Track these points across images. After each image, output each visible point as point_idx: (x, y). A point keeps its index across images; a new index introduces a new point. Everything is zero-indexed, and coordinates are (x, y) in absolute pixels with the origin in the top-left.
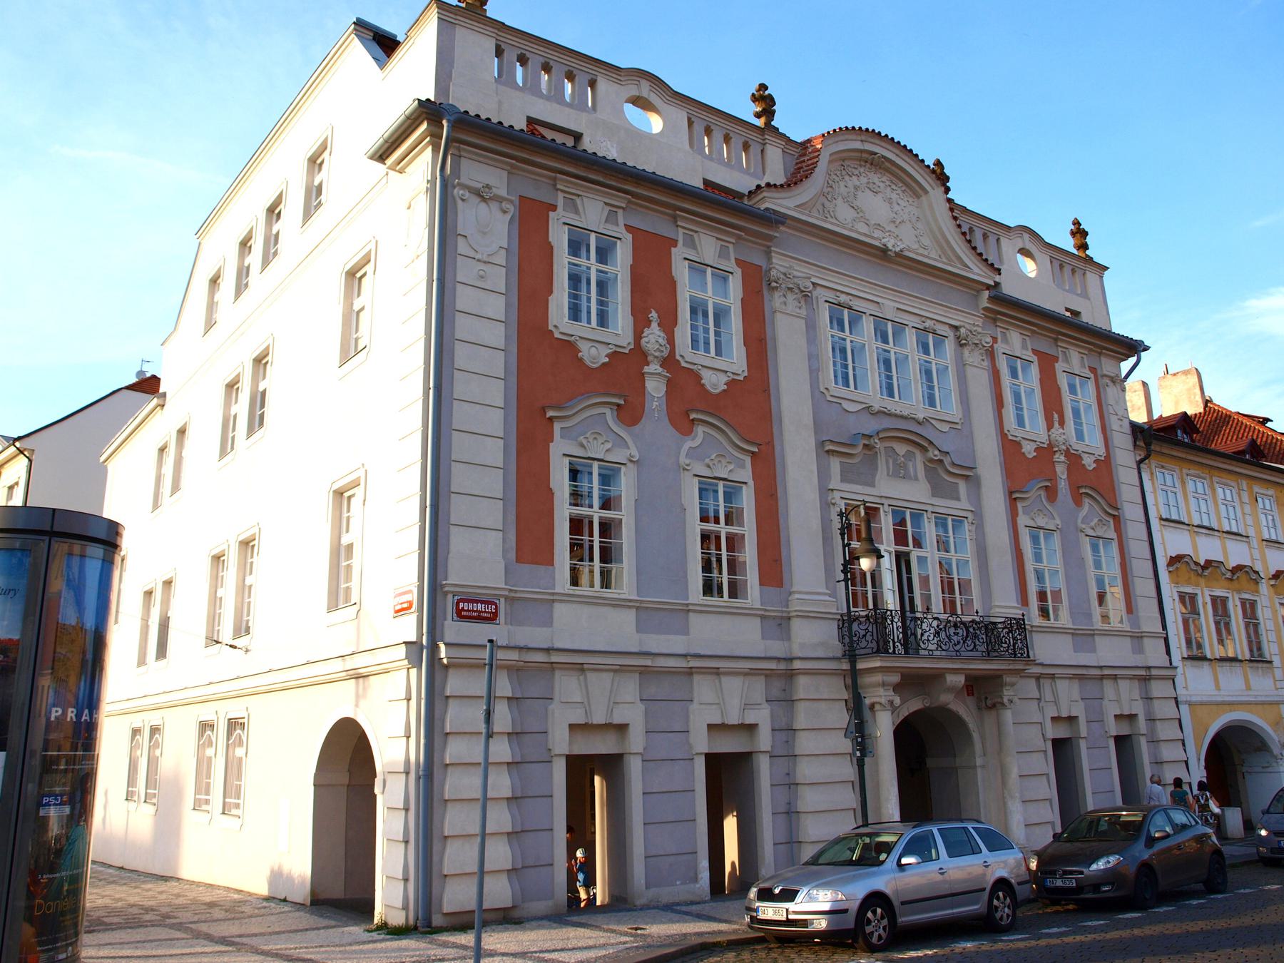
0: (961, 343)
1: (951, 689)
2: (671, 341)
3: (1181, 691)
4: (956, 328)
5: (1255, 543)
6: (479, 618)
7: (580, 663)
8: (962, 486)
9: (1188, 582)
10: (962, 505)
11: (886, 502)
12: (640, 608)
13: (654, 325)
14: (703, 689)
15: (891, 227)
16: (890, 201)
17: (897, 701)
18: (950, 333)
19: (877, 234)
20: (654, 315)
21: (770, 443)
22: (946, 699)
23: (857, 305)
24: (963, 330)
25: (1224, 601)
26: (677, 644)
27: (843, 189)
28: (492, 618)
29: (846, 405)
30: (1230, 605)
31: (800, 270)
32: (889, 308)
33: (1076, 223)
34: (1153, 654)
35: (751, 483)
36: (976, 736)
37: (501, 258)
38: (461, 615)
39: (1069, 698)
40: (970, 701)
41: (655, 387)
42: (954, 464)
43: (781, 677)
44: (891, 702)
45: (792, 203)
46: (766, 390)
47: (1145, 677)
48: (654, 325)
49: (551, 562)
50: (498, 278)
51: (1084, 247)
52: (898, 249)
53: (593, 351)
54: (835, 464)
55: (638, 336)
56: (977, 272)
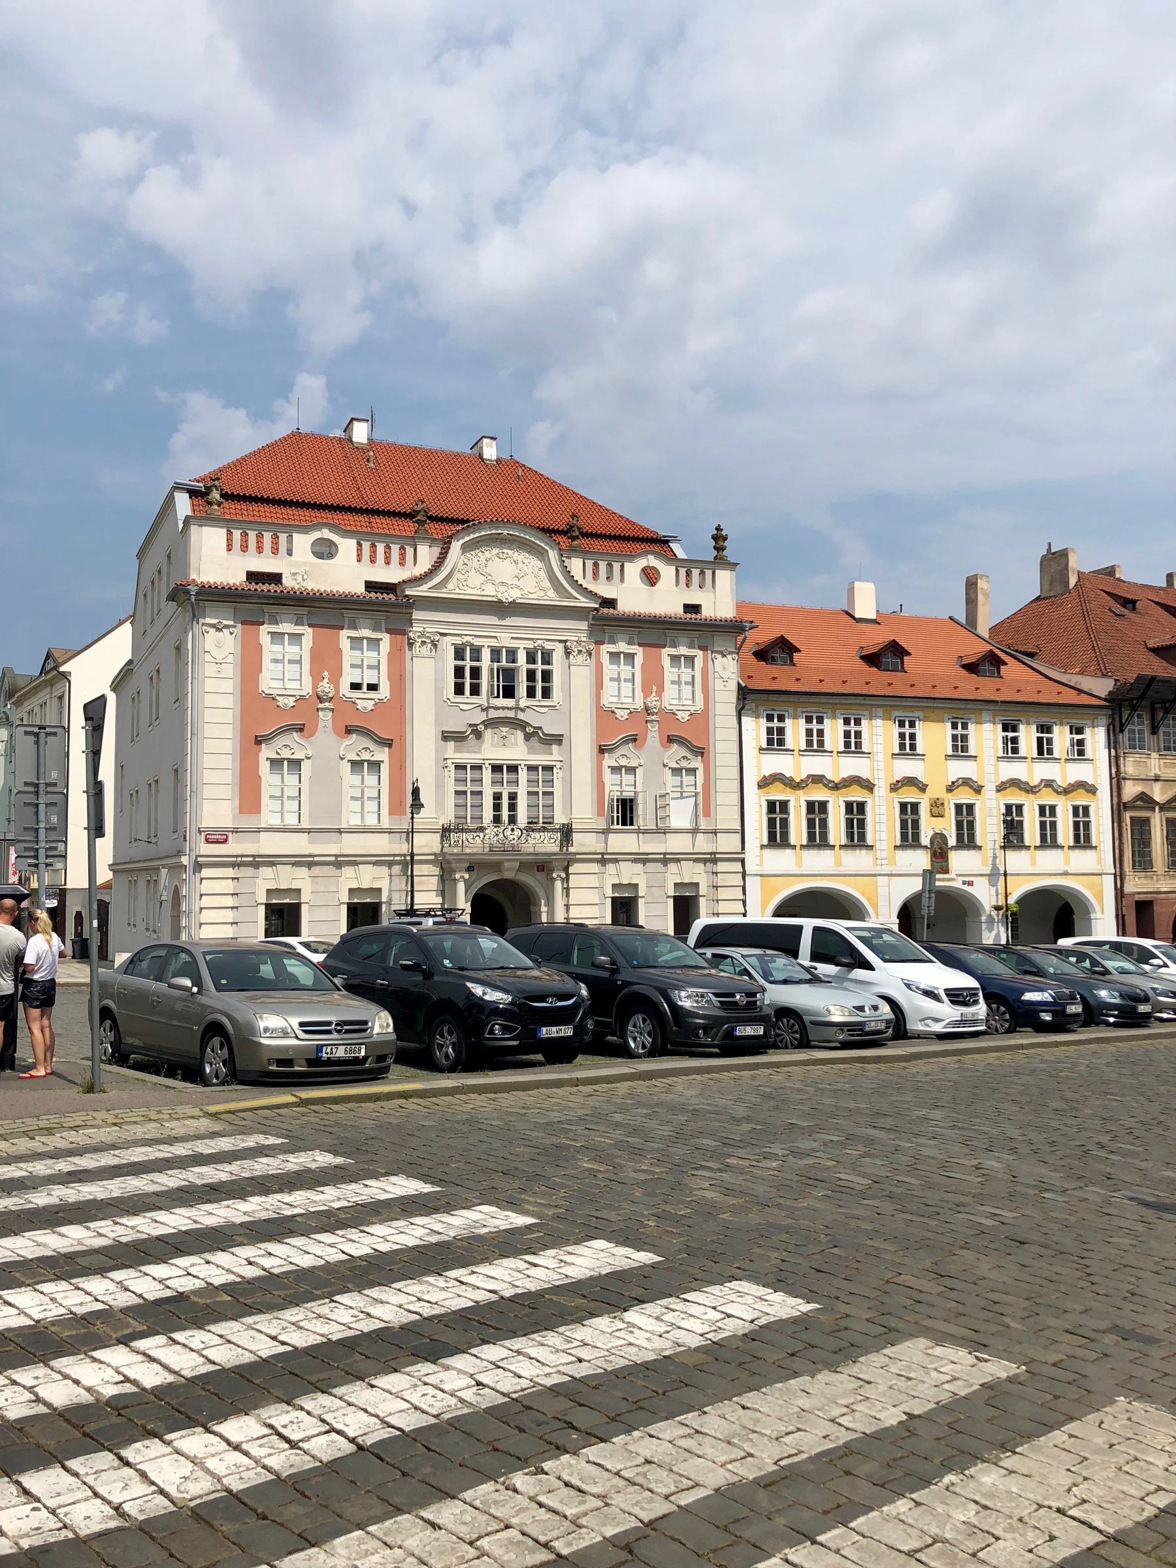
0: (568, 653)
1: (509, 869)
2: (337, 689)
3: (749, 868)
4: (565, 641)
5: (881, 757)
6: (217, 842)
7: (272, 861)
8: (555, 748)
9: (783, 792)
10: (554, 755)
11: (487, 762)
12: (309, 831)
13: (326, 680)
14: (348, 871)
15: (515, 581)
16: (516, 562)
17: (467, 876)
18: (561, 646)
19: (502, 588)
20: (326, 674)
21: (402, 738)
22: (508, 875)
23: (477, 642)
24: (568, 644)
25: (823, 806)
26: (334, 849)
27: (476, 564)
28: (225, 841)
29: (463, 707)
30: (830, 807)
31: (431, 629)
32: (505, 640)
33: (718, 529)
34: (727, 843)
35: (386, 760)
36: (541, 894)
37: (230, 659)
38: (208, 841)
39: (629, 873)
40: (541, 876)
41: (325, 717)
42: (544, 734)
43: (408, 862)
44: (462, 877)
45: (425, 587)
46: (402, 708)
47: (712, 859)
48: (326, 680)
49: (259, 812)
50: (229, 670)
51: (720, 549)
52: (510, 600)
53: (286, 701)
54: (451, 744)
55: (315, 687)
56: (584, 602)
